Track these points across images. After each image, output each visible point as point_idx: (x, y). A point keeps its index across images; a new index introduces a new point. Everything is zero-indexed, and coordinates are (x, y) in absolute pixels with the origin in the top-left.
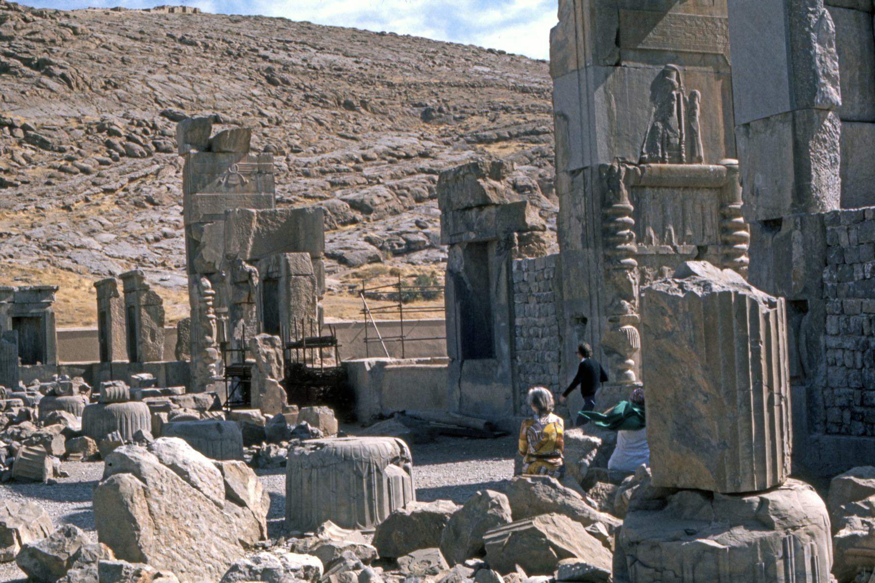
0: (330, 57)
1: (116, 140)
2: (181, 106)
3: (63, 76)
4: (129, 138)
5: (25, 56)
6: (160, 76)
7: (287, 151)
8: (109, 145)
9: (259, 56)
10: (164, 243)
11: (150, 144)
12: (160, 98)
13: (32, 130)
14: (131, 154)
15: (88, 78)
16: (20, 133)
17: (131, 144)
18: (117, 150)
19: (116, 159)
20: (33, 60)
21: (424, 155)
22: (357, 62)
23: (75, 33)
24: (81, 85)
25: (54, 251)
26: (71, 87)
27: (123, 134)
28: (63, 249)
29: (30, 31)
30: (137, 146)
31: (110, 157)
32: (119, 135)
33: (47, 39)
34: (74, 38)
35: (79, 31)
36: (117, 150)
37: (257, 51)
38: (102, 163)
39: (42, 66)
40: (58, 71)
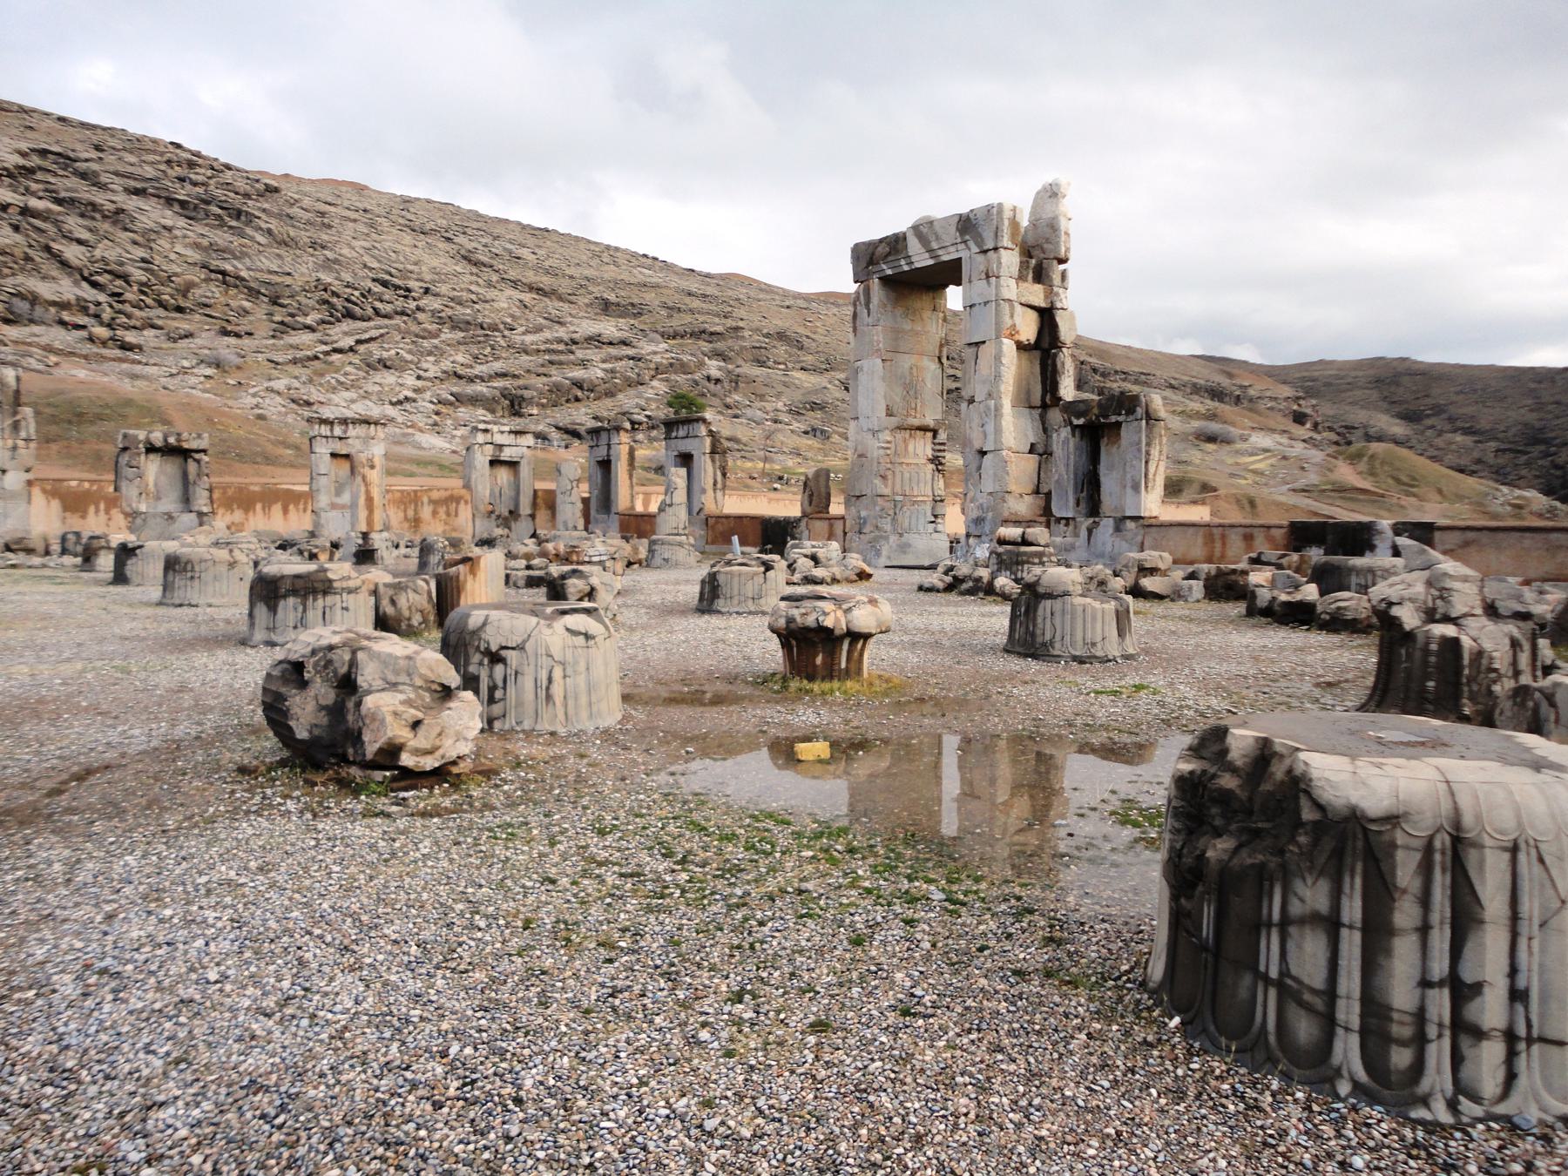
7: (502, 327)
10: (407, 406)
19: (339, 321)
21: (624, 343)
30: (357, 309)
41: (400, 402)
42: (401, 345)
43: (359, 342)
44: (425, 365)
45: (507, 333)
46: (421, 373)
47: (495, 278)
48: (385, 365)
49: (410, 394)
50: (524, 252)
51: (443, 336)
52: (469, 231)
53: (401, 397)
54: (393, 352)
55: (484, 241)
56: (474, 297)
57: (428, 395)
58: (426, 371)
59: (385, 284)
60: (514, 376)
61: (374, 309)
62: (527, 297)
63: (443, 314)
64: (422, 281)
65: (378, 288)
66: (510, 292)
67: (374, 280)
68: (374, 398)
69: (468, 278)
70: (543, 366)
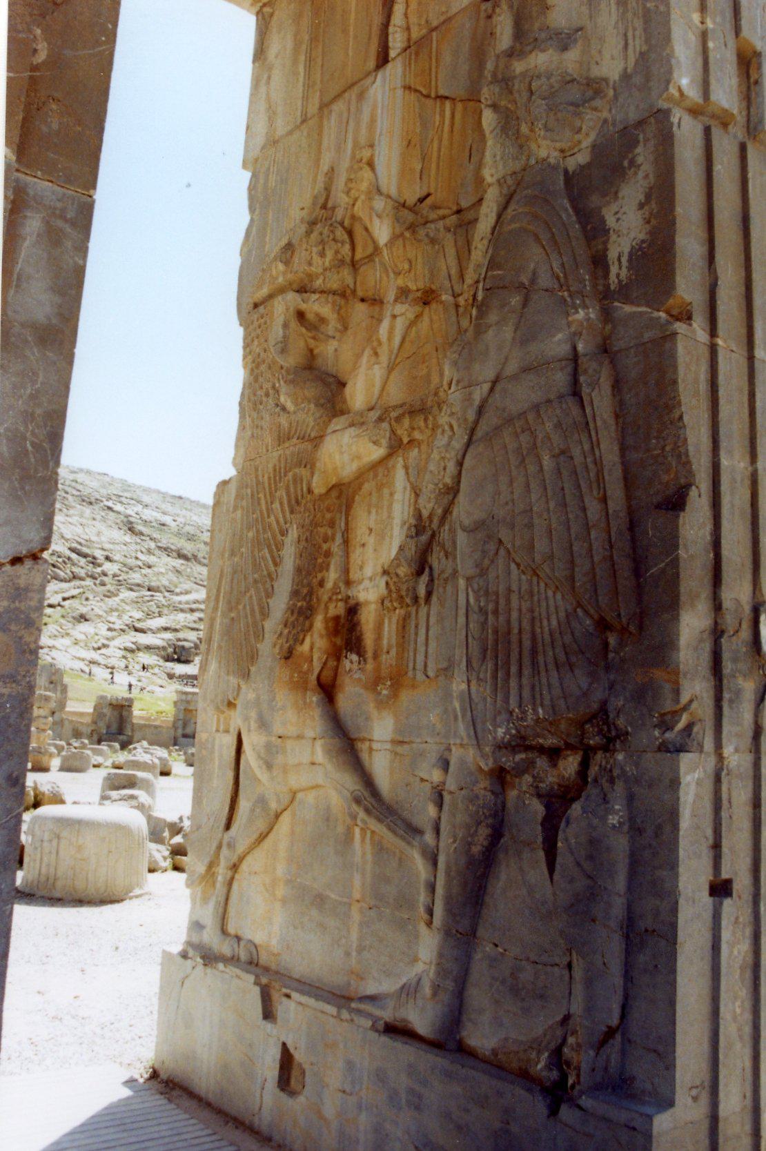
0: (155, 514)
2: (80, 544)
7: (163, 590)
10: (103, 651)
17: (56, 570)
22: (174, 521)
41: (99, 648)
43: (64, 599)
44: (112, 619)
45: (167, 594)
46: (111, 625)
47: (153, 545)
48: (83, 618)
49: (106, 642)
50: (167, 519)
51: (122, 596)
52: (123, 499)
53: (100, 644)
54: (89, 608)
56: (140, 563)
58: (113, 623)
59: (79, 554)
60: (176, 630)
61: (72, 573)
62: (178, 563)
63: (120, 578)
64: (104, 550)
65: (74, 556)
66: (166, 559)
67: (70, 549)
68: (82, 644)
69: (134, 547)
70: (195, 622)
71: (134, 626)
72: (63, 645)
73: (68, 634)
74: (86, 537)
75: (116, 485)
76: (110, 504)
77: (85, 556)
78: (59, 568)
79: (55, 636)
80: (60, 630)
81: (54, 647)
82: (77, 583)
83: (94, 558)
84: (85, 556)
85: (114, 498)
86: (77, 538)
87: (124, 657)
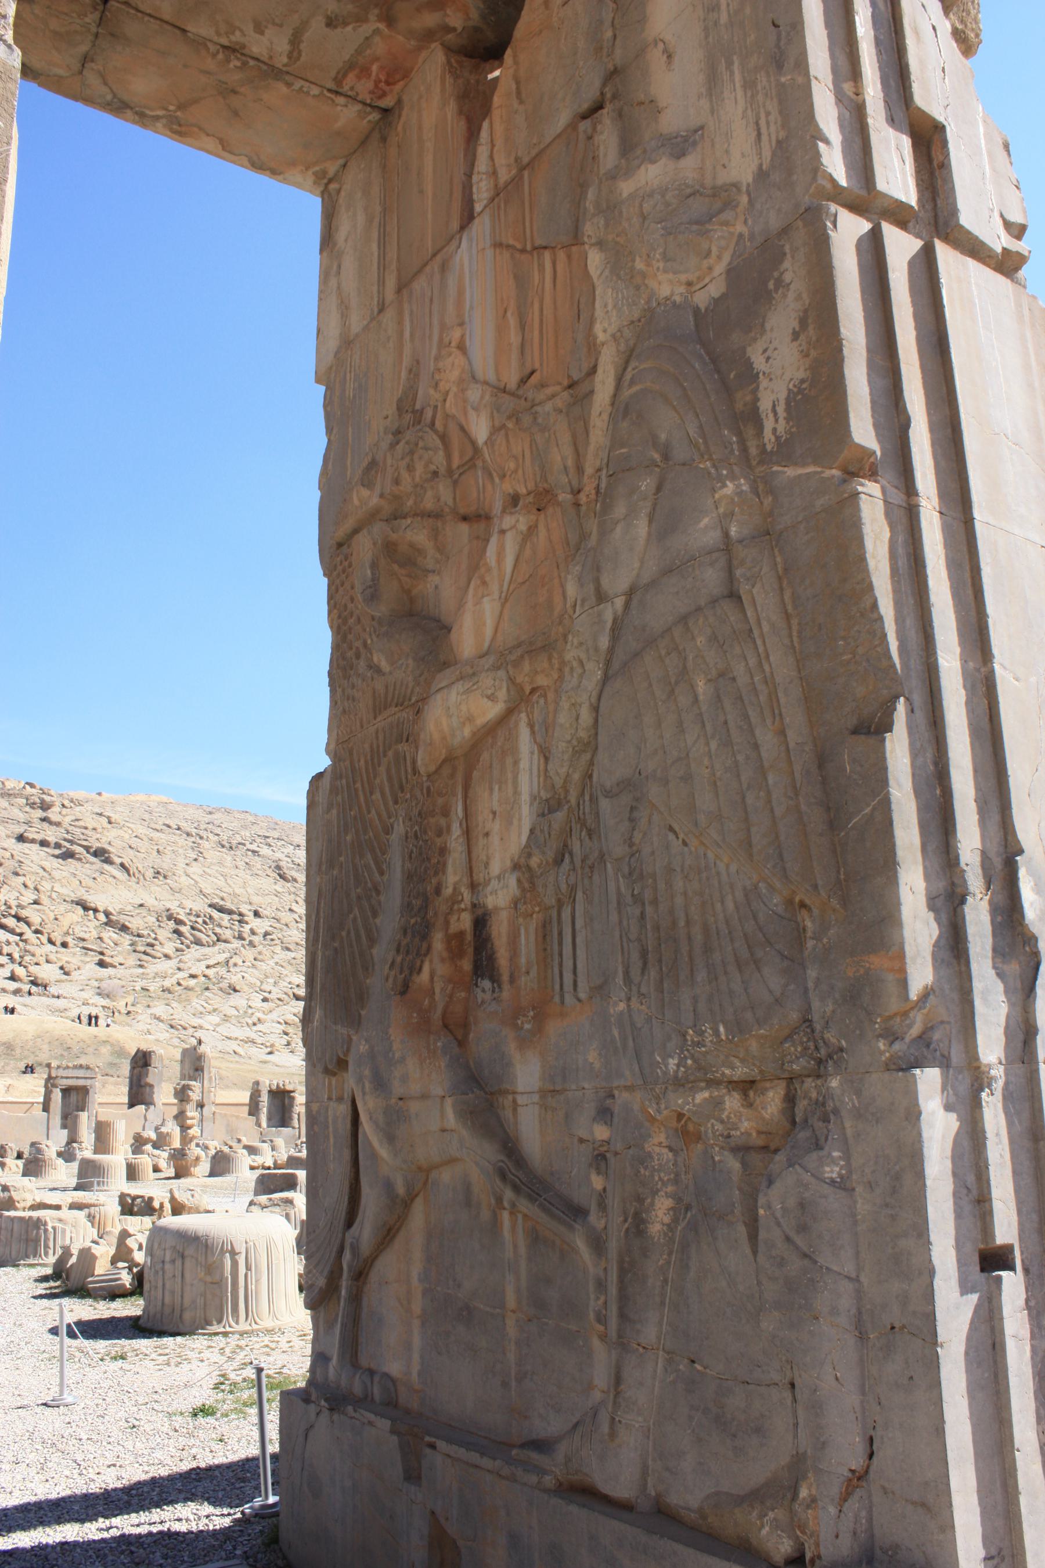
1: (183, 929)
2: (222, 899)
3: (122, 865)
4: (193, 928)
5: (85, 843)
6: (195, 869)
8: (176, 932)
9: (248, 850)
10: (259, 1027)
11: (210, 933)
12: (204, 890)
13: (111, 914)
14: (198, 942)
15: (140, 868)
16: (102, 918)
17: (196, 932)
18: (186, 938)
19: (188, 947)
20: (91, 847)
23: (110, 822)
24: (137, 875)
25: (178, 1029)
26: (129, 875)
27: (188, 923)
28: (185, 1029)
29: (74, 818)
31: (182, 943)
32: (185, 924)
33: (90, 827)
34: (109, 826)
35: (113, 820)
36: (186, 938)
37: (244, 845)
38: (177, 950)
39: (100, 854)
40: (118, 861)
42: (244, 969)
43: (208, 967)
46: (266, 995)
55: (286, 851)
57: (274, 1016)
59: (221, 910)
61: (215, 934)
65: (216, 914)
71: (294, 995)
72: (211, 1024)
73: (215, 1010)
74: (230, 890)
75: (262, 824)
76: (254, 847)
77: (230, 912)
78: (200, 931)
79: (201, 1013)
80: (206, 1005)
81: (201, 1027)
82: (222, 945)
83: (241, 914)
84: (230, 912)
85: (258, 840)
86: (218, 892)
87: (286, 1034)
